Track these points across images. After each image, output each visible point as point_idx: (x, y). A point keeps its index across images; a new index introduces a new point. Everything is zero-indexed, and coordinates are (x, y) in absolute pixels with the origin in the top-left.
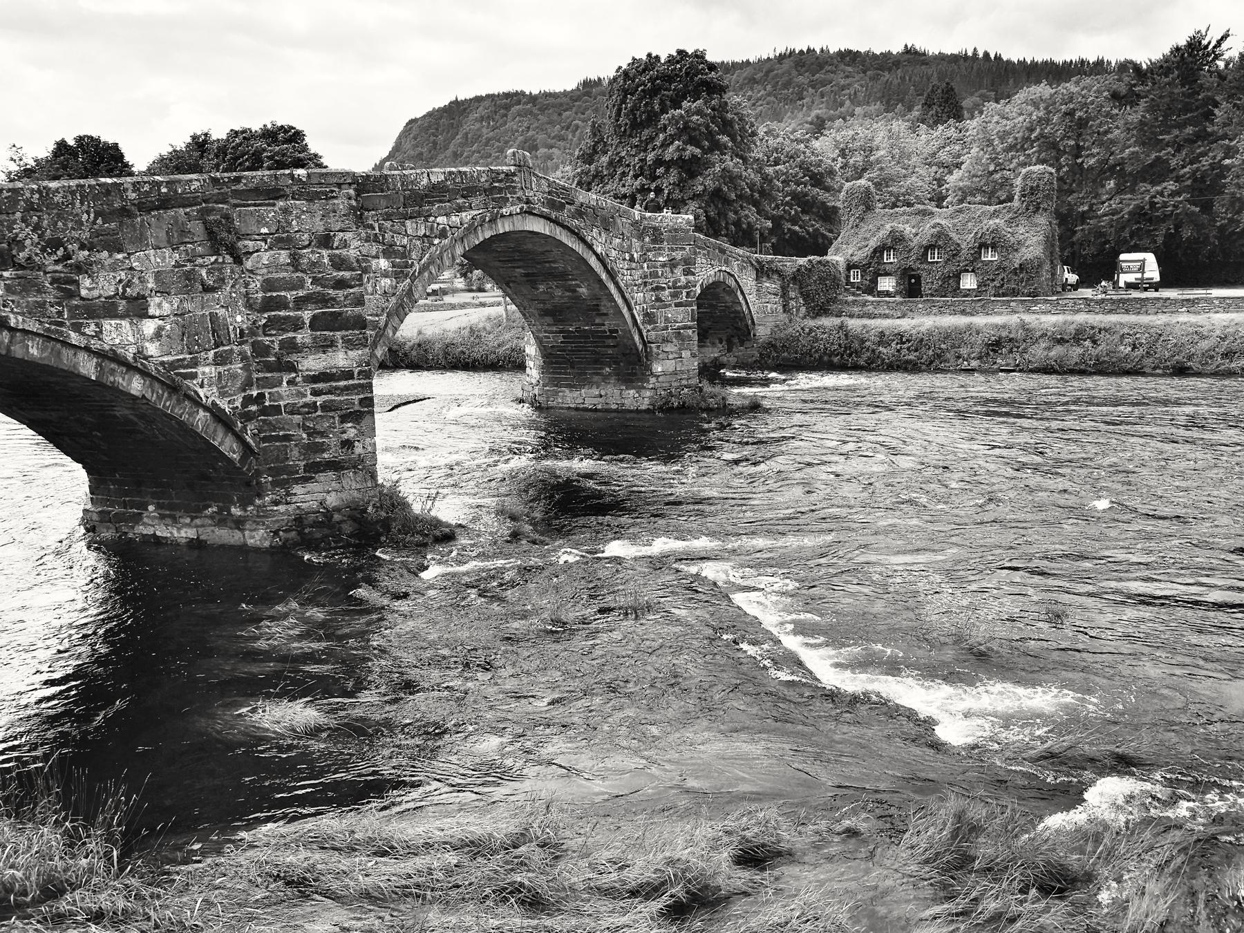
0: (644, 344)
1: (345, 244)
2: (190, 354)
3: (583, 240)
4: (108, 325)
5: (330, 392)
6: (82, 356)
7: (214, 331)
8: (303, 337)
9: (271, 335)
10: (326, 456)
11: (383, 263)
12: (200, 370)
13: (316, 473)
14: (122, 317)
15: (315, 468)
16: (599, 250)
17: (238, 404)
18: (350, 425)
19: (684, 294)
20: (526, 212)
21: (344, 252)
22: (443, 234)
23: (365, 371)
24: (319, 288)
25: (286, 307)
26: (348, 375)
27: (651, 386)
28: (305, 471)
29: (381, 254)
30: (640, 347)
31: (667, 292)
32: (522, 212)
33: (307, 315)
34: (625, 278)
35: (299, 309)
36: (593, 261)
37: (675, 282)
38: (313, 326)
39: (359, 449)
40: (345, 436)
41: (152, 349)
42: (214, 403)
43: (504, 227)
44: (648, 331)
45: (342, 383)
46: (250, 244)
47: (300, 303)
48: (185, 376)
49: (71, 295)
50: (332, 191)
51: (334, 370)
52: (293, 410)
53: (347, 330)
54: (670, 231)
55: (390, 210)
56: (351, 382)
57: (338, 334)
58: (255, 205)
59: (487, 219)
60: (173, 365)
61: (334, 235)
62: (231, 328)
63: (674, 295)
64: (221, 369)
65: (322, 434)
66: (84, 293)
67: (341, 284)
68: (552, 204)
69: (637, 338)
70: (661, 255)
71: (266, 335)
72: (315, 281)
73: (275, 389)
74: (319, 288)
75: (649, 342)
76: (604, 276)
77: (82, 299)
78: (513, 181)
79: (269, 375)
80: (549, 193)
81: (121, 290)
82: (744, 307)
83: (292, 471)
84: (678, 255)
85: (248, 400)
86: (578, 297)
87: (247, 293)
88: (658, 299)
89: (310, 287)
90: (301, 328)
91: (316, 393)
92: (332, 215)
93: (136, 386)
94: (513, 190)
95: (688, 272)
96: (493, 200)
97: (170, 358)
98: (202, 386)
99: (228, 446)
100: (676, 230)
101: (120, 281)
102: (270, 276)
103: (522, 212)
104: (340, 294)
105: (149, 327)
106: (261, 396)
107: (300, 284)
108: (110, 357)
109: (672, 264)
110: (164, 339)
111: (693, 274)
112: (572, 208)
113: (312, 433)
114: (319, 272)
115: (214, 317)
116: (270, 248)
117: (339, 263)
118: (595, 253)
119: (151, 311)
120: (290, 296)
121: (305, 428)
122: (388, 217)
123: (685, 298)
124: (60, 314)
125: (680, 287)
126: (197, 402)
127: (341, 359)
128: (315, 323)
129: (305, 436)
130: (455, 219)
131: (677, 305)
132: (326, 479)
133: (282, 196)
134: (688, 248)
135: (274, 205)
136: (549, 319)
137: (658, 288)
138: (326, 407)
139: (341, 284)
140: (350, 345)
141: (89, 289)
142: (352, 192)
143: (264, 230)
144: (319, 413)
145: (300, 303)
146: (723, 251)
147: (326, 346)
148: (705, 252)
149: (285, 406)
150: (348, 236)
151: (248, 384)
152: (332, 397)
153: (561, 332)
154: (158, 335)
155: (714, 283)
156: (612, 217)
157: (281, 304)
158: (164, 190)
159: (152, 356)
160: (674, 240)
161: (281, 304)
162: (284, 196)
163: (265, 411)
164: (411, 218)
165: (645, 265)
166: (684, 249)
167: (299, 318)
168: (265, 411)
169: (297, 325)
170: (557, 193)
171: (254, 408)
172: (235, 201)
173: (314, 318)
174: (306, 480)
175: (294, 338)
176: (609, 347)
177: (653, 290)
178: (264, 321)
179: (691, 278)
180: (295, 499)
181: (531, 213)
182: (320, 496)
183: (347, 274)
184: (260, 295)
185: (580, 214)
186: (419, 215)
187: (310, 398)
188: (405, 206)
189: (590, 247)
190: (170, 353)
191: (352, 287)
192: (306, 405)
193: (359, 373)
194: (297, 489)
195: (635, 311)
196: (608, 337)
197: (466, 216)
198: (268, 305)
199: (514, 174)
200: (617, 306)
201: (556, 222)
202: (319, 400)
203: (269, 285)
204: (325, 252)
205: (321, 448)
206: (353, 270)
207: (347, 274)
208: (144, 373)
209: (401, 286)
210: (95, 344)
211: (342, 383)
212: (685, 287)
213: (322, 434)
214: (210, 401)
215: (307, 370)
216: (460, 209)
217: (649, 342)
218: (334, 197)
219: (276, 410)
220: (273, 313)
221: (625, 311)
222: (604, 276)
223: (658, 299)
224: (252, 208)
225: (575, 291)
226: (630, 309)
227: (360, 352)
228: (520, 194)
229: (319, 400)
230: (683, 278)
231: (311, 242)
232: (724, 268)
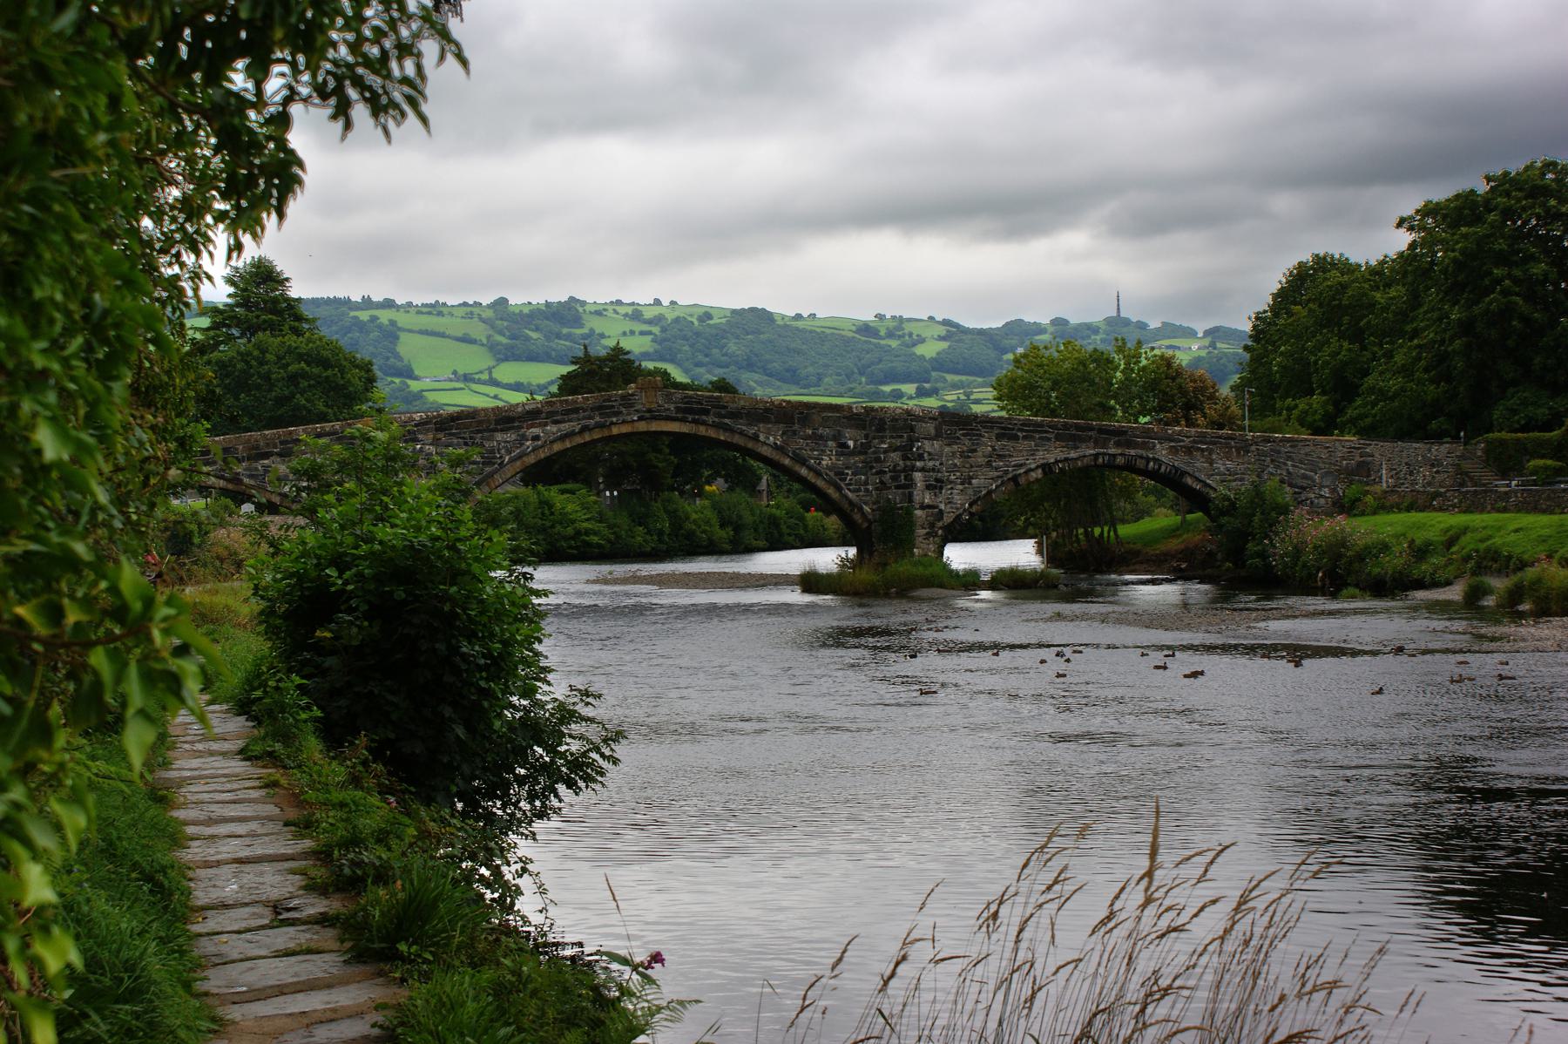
3: (741, 433)
22: (536, 438)
63: (894, 479)
70: (884, 442)
84: (898, 442)
88: (882, 482)
95: (905, 458)
103: (641, 419)
122: (479, 432)
131: (898, 487)
160: (894, 429)
166: (902, 437)
179: (908, 463)
189: (755, 438)
201: (694, 421)
212: (904, 470)
216: (556, 422)
223: (882, 482)
228: (639, 407)
230: (901, 463)
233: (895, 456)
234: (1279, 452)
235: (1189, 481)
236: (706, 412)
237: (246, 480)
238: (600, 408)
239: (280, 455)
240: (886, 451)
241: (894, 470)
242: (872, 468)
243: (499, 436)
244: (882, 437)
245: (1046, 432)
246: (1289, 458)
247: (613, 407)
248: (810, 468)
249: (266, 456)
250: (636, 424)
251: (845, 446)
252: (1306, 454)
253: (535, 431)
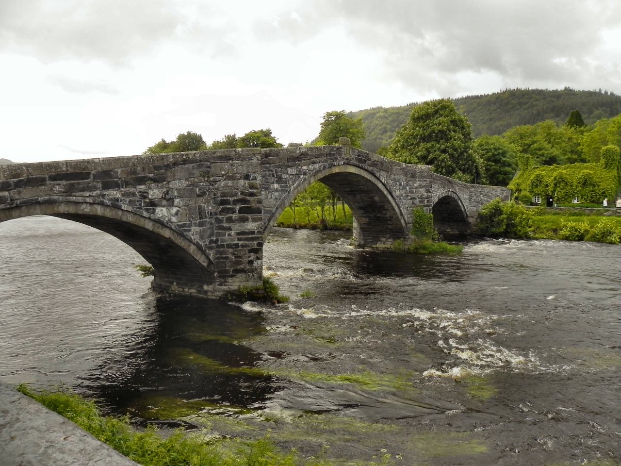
0: (406, 224)
1: (255, 178)
2: (189, 221)
4: (158, 209)
5: (245, 239)
6: (147, 221)
7: (199, 213)
8: (235, 216)
9: (223, 215)
10: (242, 266)
11: (276, 186)
12: (193, 228)
13: (237, 273)
14: (163, 206)
15: (237, 271)
16: (383, 181)
17: (207, 243)
18: (252, 254)
19: (426, 201)
20: (346, 164)
21: (254, 181)
22: (305, 174)
23: (260, 231)
24: (243, 197)
25: (229, 203)
26: (253, 233)
27: (408, 243)
28: (233, 272)
29: (275, 182)
30: (404, 225)
31: (418, 200)
32: (344, 164)
33: (238, 207)
34: (397, 193)
35: (234, 205)
36: (380, 186)
37: (422, 196)
38: (240, 212)
39: (255, 264)
40: (250, 259)
41: (174, 219)
42: (197, 242)
43: (336, 170)
44: (408, 218)
45: (250, 236)
46: (217, 178)
47: (235, 202)
48: (185, 230)
49: (145, 197)
50: (251, 157)
51: (247, 231)
52: (229, 246)
53: (254, 214)
54: (420, 172)
55: (281, 164)
56: (254, 236)
57: (250, 216)
58: (220, 163)
59: (327, 167)
60: (182, 226)
61: (251, 175)
62: (207, 212)
64: (201, 228)
65: (240, 257)
66: (150, 197)
67: (252, 195)
68: (359, 160)
69: (402, 221)
71: (221, 215)
72: (242, 193)
73: (223, 238)
74: (243, 197)
75: (408, 223)
76: (386, 192)
77: (149, 199)
78: (340, 151)
79: (220, 231)
80: (359, 156)
81: (164, 196)
82: (462, 208)
83: (228, 271)
84: (424, 184)
85: (211, 242)
86: (375, 202)
87: (215, 198)
88: (413, 203)
89: (239, 196)
90: (235, 212)
91: (239, 240)
92: (250, 166)
93: (167, 233)
94: (340, 155)
95: (428, 191)
96: (330, 159)
97: (181, 223)
98: (193, 235)
99: (202, 260)
100: (422, 172)
101: (164, 192)
102: (224, 191)
103: (344, 164)
104: (251, 199)
105: (174, 210)
106: (217, 240)
107: (236, 195)
108: (158, 222)
109: (421, 186)
110: (179, 215)
111: (430, 192)
112: (370, 162)
113: (237, 257)
114: (244, 190)
115: (200, 207)
116: (225, 180)
117: (252, 187)
118: (381, 182)
119: (175, 204)
120: (231, 199)
121: (233, 254)
122: (280, 167)
123: (426, 203)
124: (140, 205)
125: (423, 198)
126: (190, 241)
127: (251, 226)
128: (241, 211)
129: (233, 258)
130: (311, 167)
132: (241, 276)
133: (231, 159)
134: (428, 180)
135: (228, 162)
136: (362, 211)
137: (414, 198)
138: (242, 246)
139: (252, 195)
140: (254, 220)
141: (152, 195)
142: (259, 157)
143: (223, 173)
144: (240, 248)
145: (235, 202)
146: (450, 182)
147: (244, 220)
148: (440, 182)
149: (226, 245)
150: (257, 175)
151: (212, 235)
152: (246, 242)
153: (367, 217)
154: (177, 214)
155: (446, 196)
156: (391, 166)
157: (228, 202)
158: (184, 157)
159: (174, 222)
160: (422, 176)
161: (228, 202)
162: (232, 159)
163: (218, 247)
164: (290, 167)
165: (408, 188)
166: (426, 181)
167: (234, 208)
168: (218, 247)
169: (233, 211)
170: (362, 156)
171: (213, 245)
172: (212, 161)
173: (241, 208)
174: (232, 276)
175: (232, 217)
176: (389, 225)
177: (411, 199)
178: (220, 209)
179: (430, 194)
180: (228, 284)
181: (349, 164)
182: (238, 284)
183: (255, 191)
184: (219, 199)
185: (374, 164)
186: (295, 165)
187: (236, 242)
188: (288, 162)
189: (378, 179)
190: (181, 222)
191: (256, 196)
192: (235, 244)
193: (258, 232)
194: (230, 280)
195: (401, 209)
196: (388, 220)
197: (317, 166)
198: (223, 203)
199: (341, 148)
200: (392, 207)
201: (362, 168)
202: (241, 243)
203: (224, 195)
204: (246, 182)
205: (239, 263)
206: (258, 189)
207: (255, 191)
208: (171, 229)
209: (284, 196)
210: (152, 216)
211: (250, 236)
212: (427, 198)
213: (240, 257)
214: (195, 241)
215: (236, 230)
216: (313, 163)
217: (408, 223)
218: (252, 159)
219: (223, 246)
220: (224, 206)
221: (396, 208)
222: (386, 192)
224: (219, 164)
225: (373, 199)
226: (399, 208)
227: (258, 223)
228: (344, 156)
229: (241, 243)
230: (425, 194)
231: (241, 177)
232: (450, 190)
233: (422, 191)
234: (477, 191)
235: (459, 202)
236: (365, 161)
237: (124, 207)
238: (330, 154)
239: (155, 181)
240: (416, 188)
241: (421, 197)
242: (408, 196)
243: (290, 171)
244: (415, 180)
245: (440, 180)
246: (481, 194)
247: (334, 155)
248: (392, 196)
249: (141, 181)
250: (341, 167)
251: (400, 185)
252: (487, 192)
253: (305, 168)
